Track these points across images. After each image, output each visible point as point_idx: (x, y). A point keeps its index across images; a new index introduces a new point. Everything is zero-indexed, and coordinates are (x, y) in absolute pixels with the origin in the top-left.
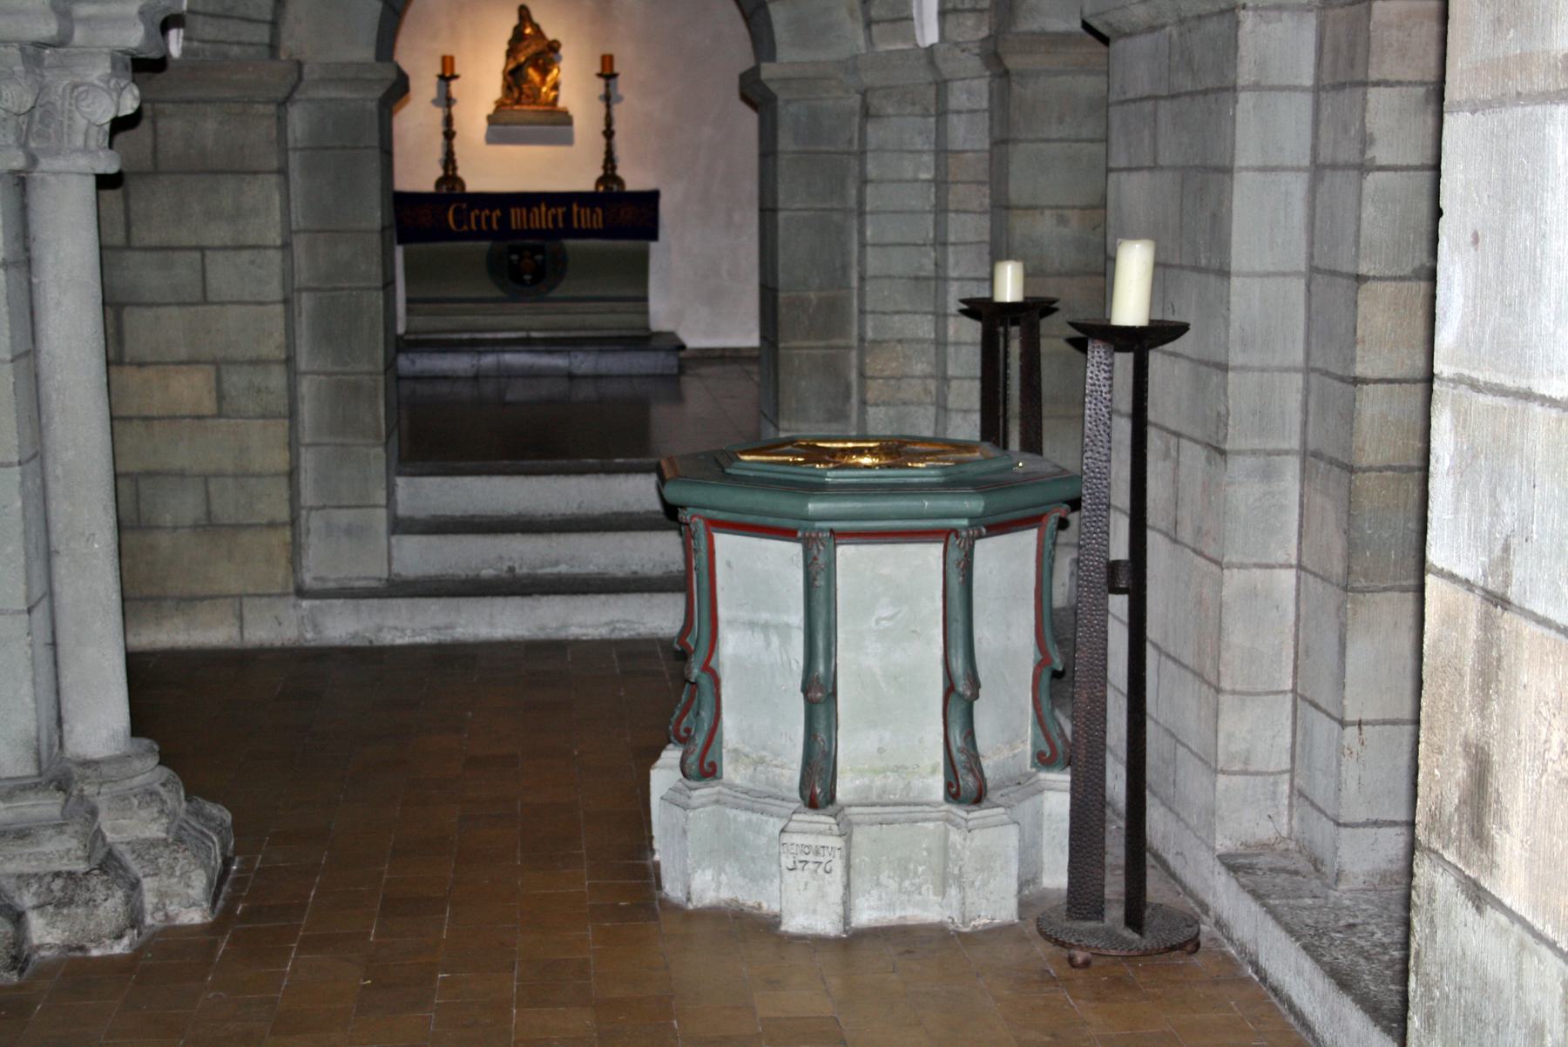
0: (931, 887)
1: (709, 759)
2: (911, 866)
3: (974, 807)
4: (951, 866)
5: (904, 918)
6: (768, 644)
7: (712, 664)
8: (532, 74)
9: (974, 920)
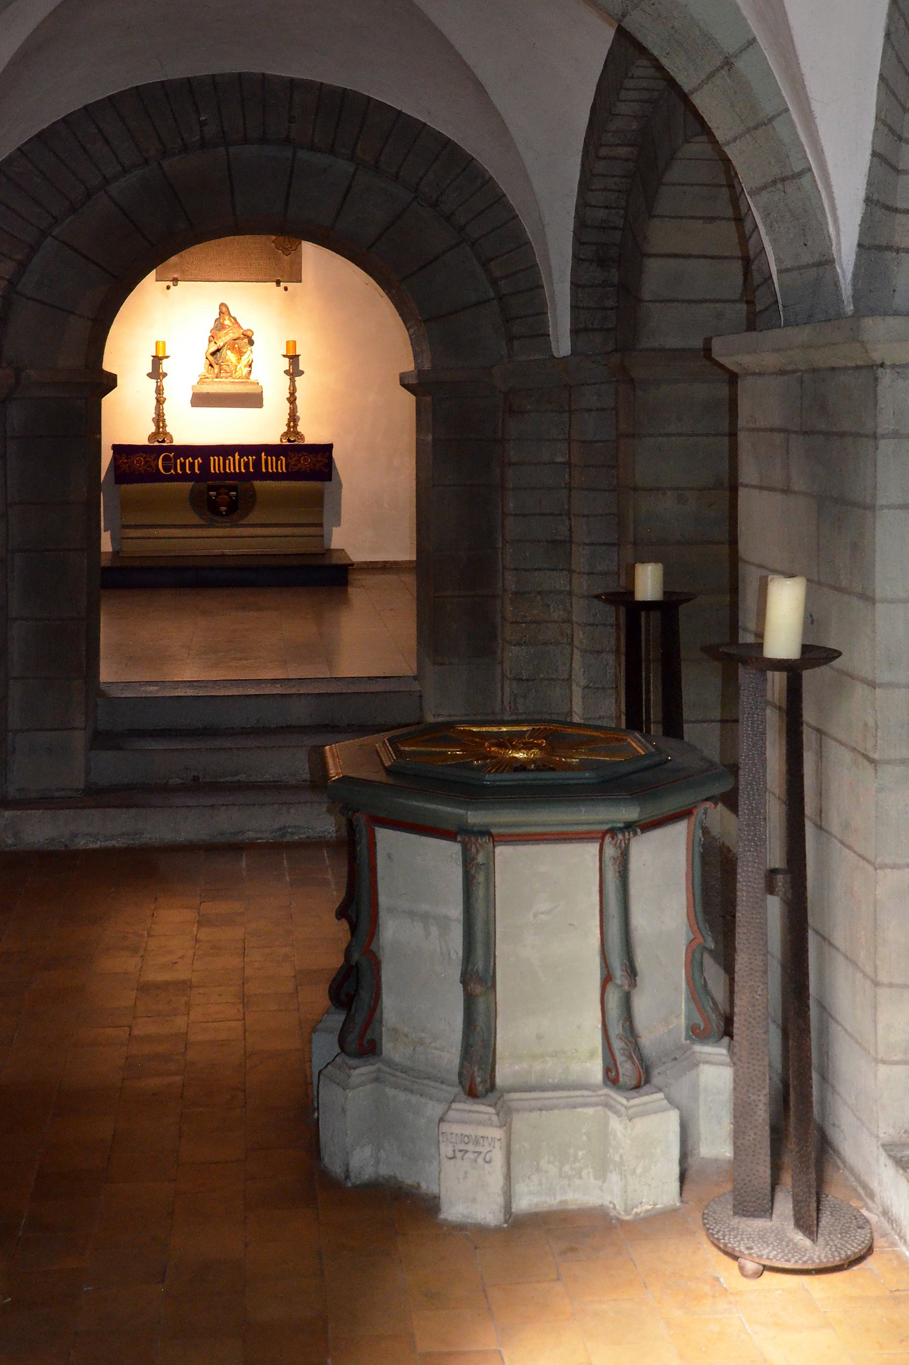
0: (591, 1170)
1: (368, 1036)
2: (572, 1151)
3: (633, 1093)
4: (611, 1151)
5: (565, 1202)
6: (428, 934)
7: (373, 947)
8: (231, 356)
9: (636, 1207)
